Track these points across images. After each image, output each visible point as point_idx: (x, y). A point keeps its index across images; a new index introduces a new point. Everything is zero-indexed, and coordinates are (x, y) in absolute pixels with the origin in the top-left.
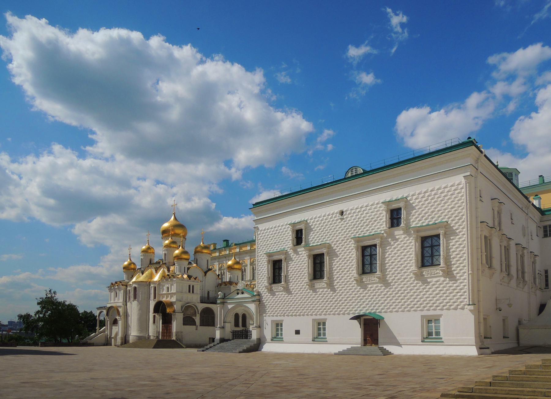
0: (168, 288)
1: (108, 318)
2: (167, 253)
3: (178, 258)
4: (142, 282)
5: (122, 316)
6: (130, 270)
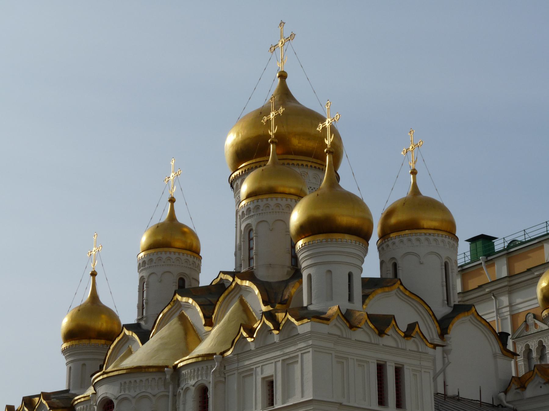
0: (270, 384)
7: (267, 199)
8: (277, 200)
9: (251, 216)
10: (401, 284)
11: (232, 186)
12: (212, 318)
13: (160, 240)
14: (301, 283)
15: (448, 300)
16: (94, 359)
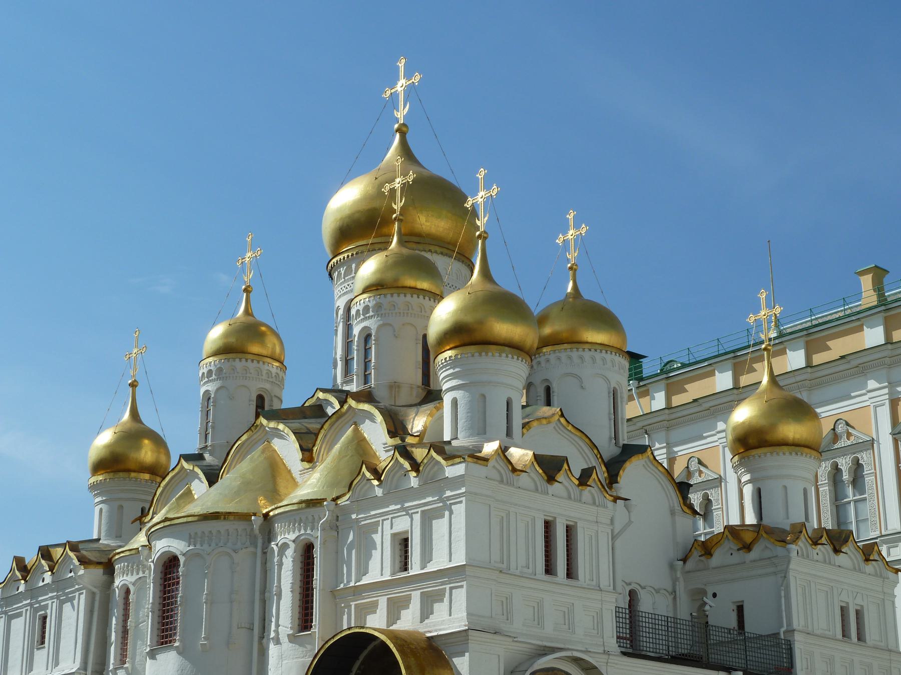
0: (403, 543)
2: (379, 329)
4: (215, 516)
6: (133, 475)
7: (392, 295)
8: (405, 296)
9: (369, 317)
11: (330, 275)
12: (312, 450)
13: (233, 343)
14: (440, 408)
15: (616, 437)
16: (134, 500)
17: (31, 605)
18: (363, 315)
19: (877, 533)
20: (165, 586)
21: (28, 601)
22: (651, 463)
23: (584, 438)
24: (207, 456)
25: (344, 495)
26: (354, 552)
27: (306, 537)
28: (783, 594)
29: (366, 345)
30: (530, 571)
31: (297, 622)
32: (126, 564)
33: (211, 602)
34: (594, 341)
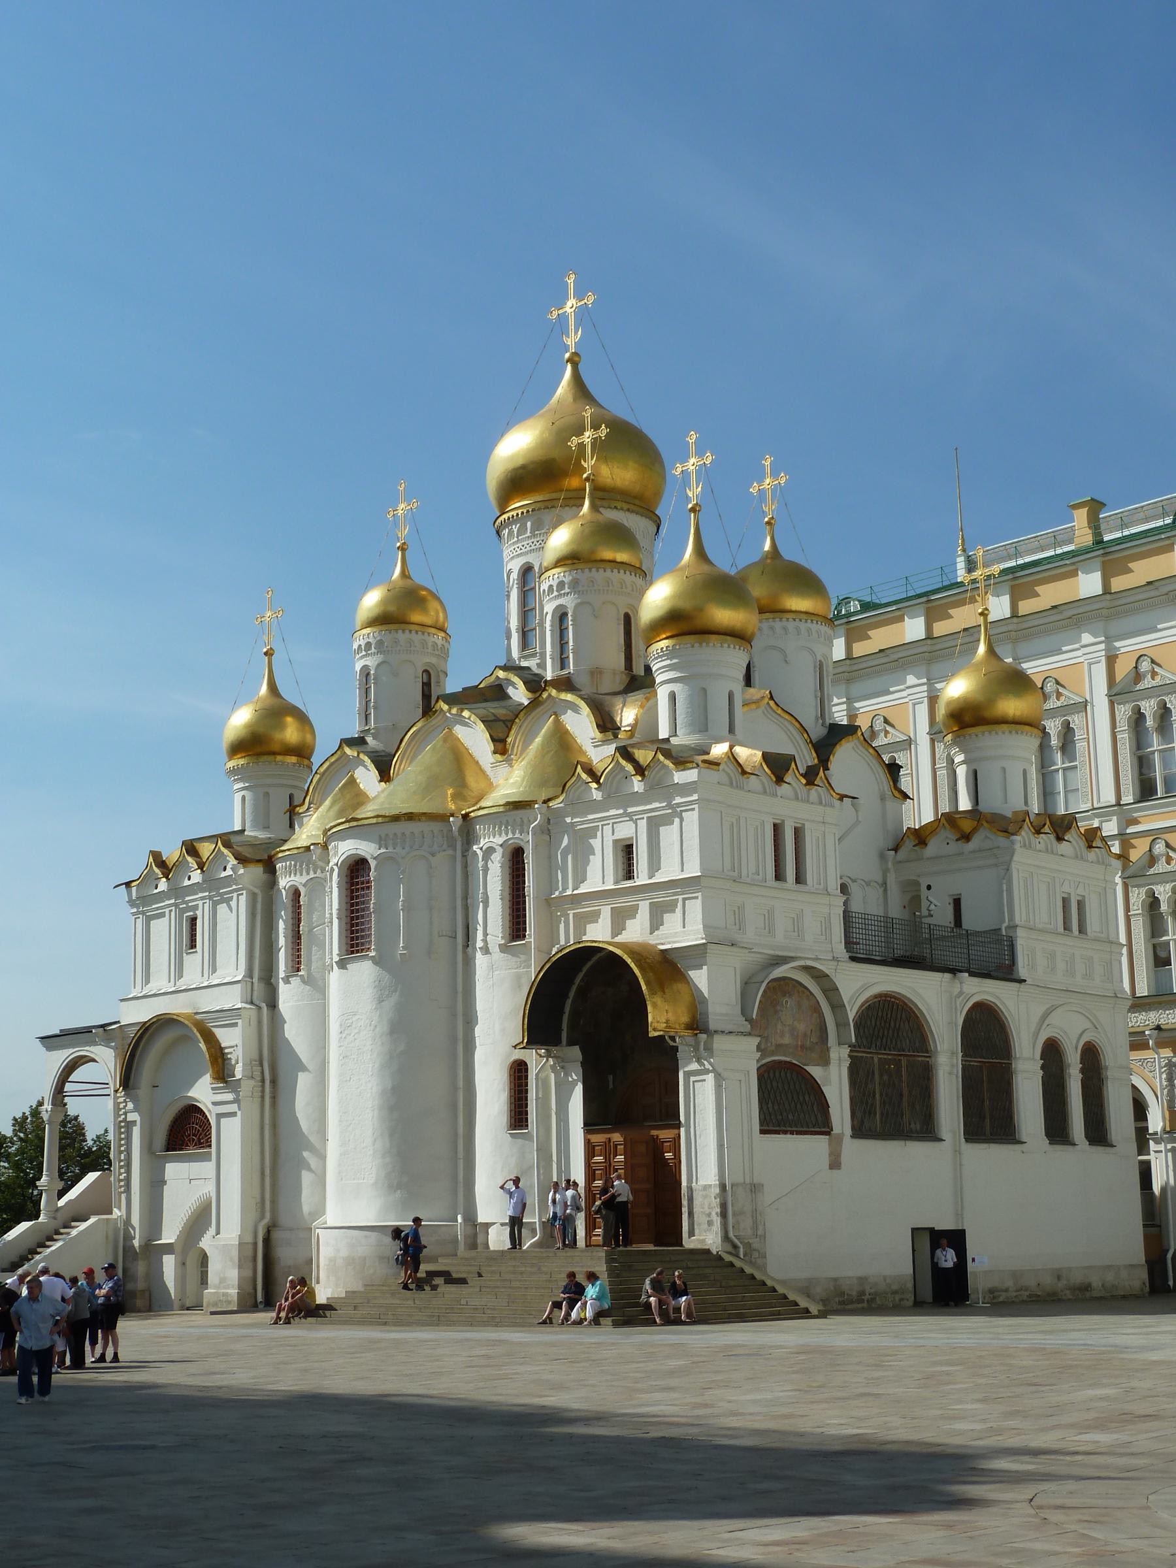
0: (627, 851)
1: (130, 1106)
2: (576, 607)
3: (684, 626)
4: (410, 817)
5: (247, 1087)
6: (279, 758)
7: (590, 569)
8: (605, 571)
9: (564, 594)
10: (772, 698)
11: (498, 532)
12: (506, 741)
16: (282, 786)
17: (176, 905)
18: (557, 591)
19: (1088, 806)
20: (352, 891)
21: (173, 901)
22: (862, 744)
23: (794, 721)
24: (369, 739)
25: (557, 797)
26: (570, 857)
27: (516, 841)
28: (1005, 887)
29: (561, 626)
30: (760, 877)
31: (508, 931)
32: (293, 863)
33: (408, 909)
34: (798, 608)
